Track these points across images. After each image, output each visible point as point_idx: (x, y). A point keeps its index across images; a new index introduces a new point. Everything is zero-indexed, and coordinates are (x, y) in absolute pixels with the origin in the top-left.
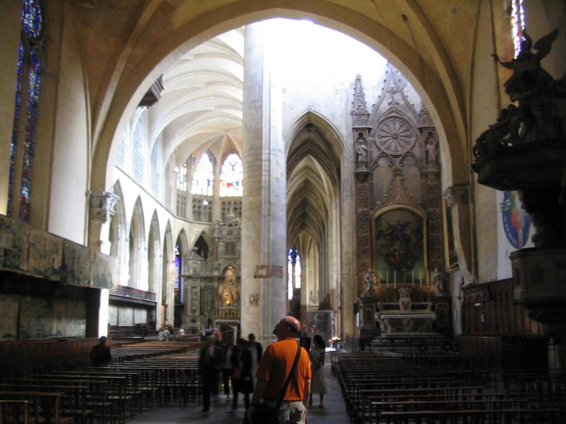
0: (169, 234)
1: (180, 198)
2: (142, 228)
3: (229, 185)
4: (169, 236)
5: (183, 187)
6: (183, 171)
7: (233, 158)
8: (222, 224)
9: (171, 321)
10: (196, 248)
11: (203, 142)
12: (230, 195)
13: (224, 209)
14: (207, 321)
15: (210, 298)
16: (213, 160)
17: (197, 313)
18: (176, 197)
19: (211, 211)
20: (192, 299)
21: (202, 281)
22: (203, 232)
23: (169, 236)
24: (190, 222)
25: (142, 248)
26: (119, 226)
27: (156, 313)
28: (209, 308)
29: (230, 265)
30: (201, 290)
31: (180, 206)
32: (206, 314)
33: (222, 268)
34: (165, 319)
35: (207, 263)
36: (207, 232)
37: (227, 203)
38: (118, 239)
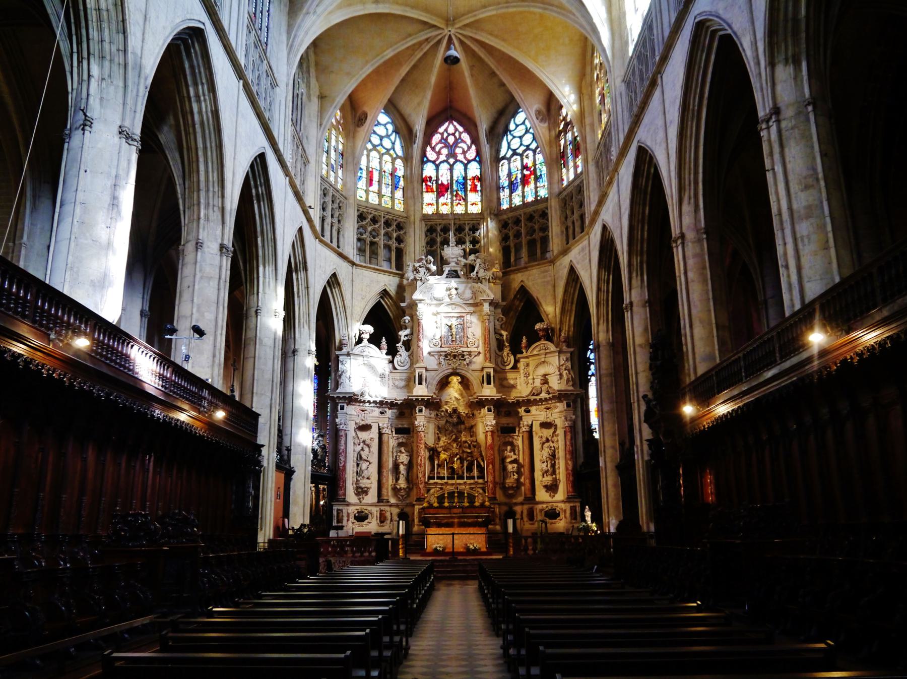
0: (301, 274)
1: (329, 199)
2: (213, 177)
3: (442, 190)
4: (302, 283)
5: (337, 179)
6: (337, 141)
7: (450, 128)
8: (434, 268)
9: (299, 517)
10: (369, 329)
11: (389, 54)
12: (445, 210)
13: (431, 243)
14: (396, 518)
15: (404, 458)
16: (404, 130)
17: (372, 497)
18: (319, 192)
19: (402, 245)
20: (360, 457)
21: (381, 413)
22: (385, 293)
23: (302, 283)
24: (353, 264)
25: (211, 247)
26: (95, 70)
27: (257, 488)
28: (402, 483)
29: (455, 373)
30: (381, 435)
31: (328, 220)
32: (393, 501)
33: (434, 378)
34: (285, 510)
35: (395, 368)
36: (392, 290)
37: (439, 229)
38: (87, 123)
